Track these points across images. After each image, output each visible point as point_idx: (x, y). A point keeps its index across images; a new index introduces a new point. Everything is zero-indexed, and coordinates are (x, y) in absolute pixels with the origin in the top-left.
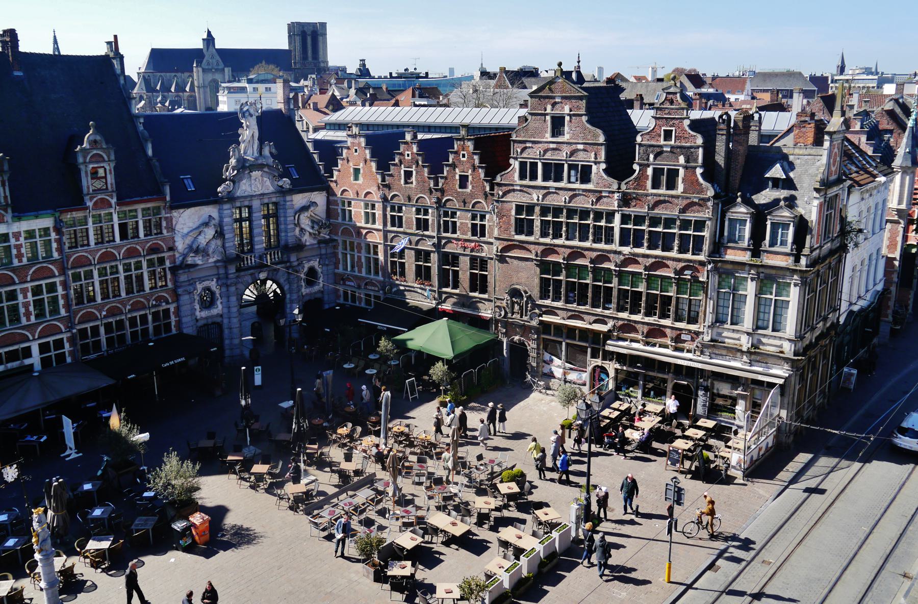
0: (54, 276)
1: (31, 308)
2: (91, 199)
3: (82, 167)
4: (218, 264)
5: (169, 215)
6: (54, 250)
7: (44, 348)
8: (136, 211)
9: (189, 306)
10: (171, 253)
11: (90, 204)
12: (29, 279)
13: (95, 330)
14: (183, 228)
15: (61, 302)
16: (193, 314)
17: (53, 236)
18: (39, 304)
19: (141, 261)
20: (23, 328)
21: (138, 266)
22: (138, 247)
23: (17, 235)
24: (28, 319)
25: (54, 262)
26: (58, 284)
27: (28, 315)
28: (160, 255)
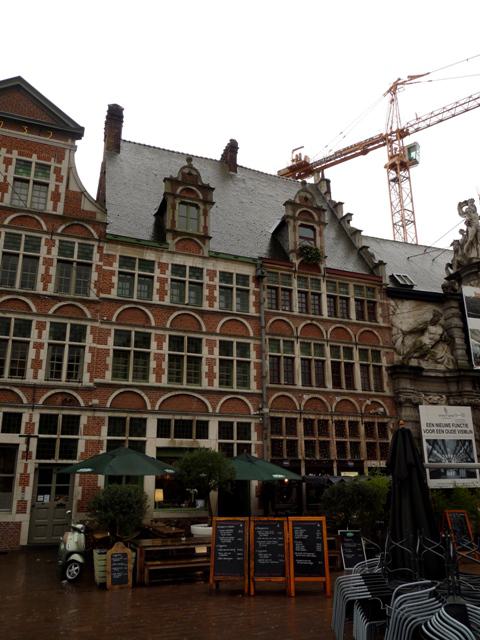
0: (249, 338)
1: (216, 369)
4: (448, 375)
6: (251, 304)
7: (225, 430)
13: (292, 422)
15: (253, 372)
17: (252, 286)
18: (225, 365)
21: (349, 352)
23: (212, 274)
25: (248, 318)
26: (252, 346)
27: (210, 375)
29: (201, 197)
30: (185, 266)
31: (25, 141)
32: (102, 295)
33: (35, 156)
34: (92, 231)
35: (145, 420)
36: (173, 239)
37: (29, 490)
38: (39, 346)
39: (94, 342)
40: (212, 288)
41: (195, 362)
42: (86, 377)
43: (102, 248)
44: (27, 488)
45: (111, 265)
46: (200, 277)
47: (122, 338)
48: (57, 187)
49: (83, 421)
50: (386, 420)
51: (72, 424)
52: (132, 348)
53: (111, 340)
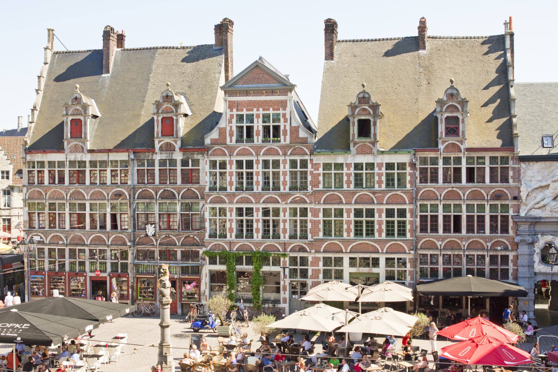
0: (405, 203)
2: (443, 142)
3: (439, 116)
5: (516, 166)
8: (483, 158)
9: (526, 257)
10: (515, 202)
11: (441, 147)
12: (385, 202)
14: (531, 181)
15: (408, 227)
16: (531, 266)
17: (408, 170)
19: (484, 205)
20: (376, 241)
22: (483, 191)
23: (380, 165)
24: (380, 235)
28: (504, 202)
29: (372, 112)
30: (362, 164)
31: (265, 101)
32: (314, 189)
33: (271, 109)
34: (306, 150)
35: (342, 258)
36: (354, 147)
37: (287, 293)
38: (285, 221)
39: (312, 216)
40: (380, 175)
41: (370, 225)
42: (309, 236)
43: (313, 159)
44: (286, 292)
45: (318, 170)
46: (373, 169)
47: (326, 213)
48: (285, 126)
49: (310, 259)
50: (507, 253)
51: (304, 261)
52: (333, 218)
53: (321, 214)
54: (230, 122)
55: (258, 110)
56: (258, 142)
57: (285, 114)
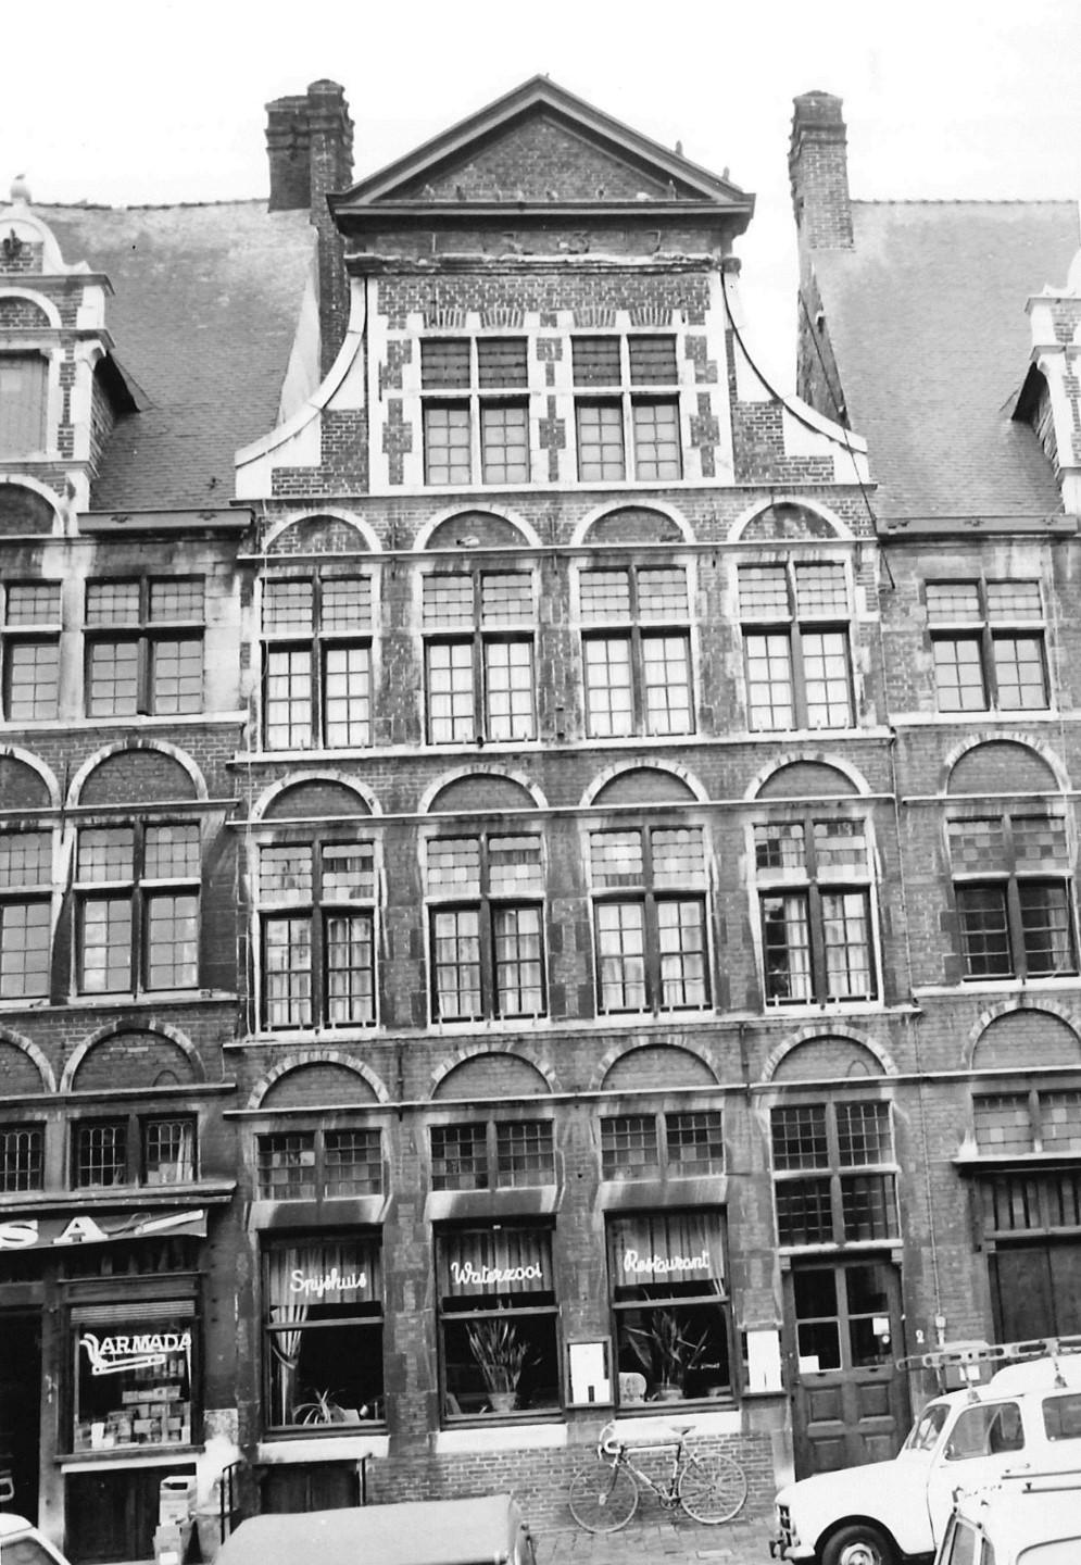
48: (704, 401)
54: (390, 378)
55: (550, 320)
56: (553, 476)
57: (703, 341)
